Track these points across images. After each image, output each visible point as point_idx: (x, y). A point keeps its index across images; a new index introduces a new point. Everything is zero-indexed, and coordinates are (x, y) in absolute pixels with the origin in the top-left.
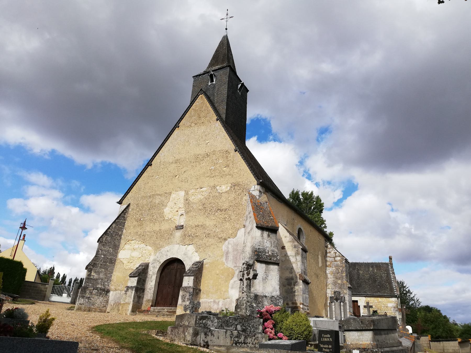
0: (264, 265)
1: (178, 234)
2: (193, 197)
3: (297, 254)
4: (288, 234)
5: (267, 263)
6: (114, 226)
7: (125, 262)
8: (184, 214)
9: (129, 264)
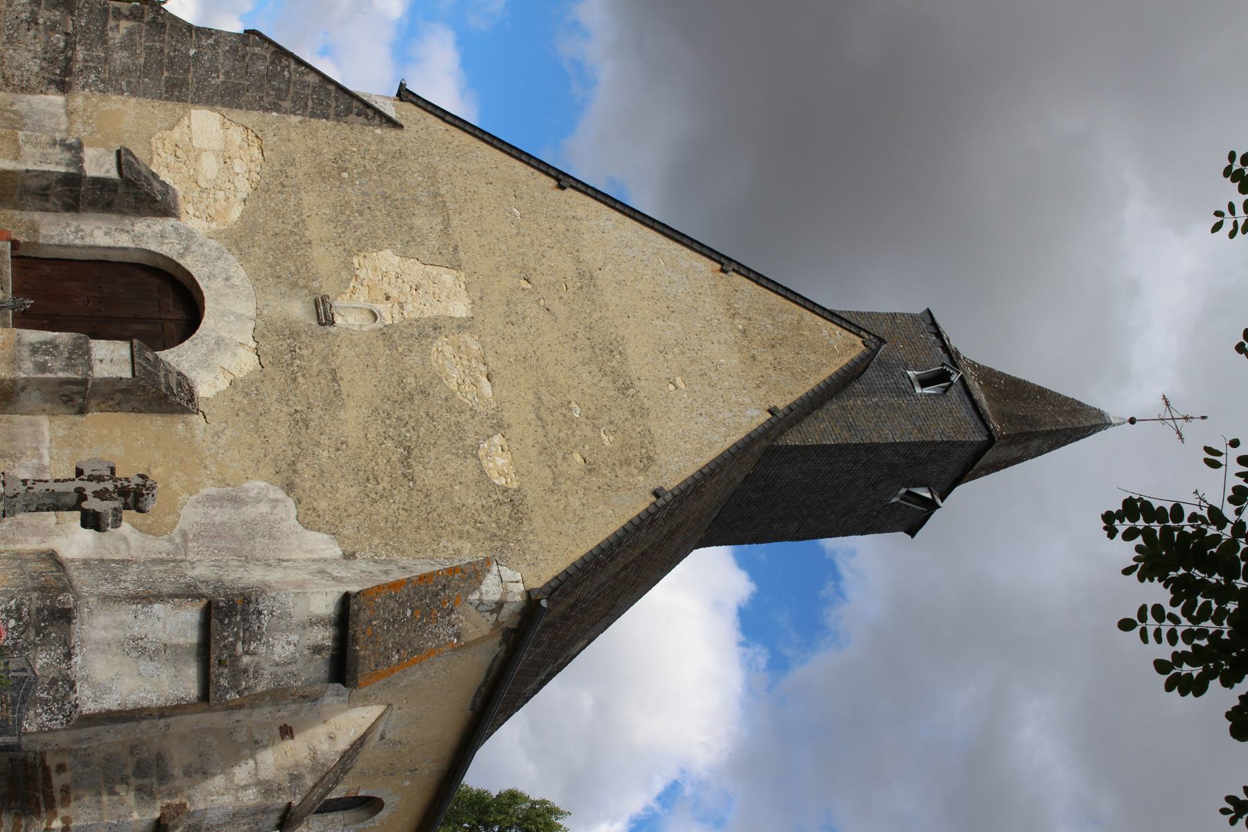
0: (192, 637)
1: (299, 310)
2: (448, 350)
3: (267, 788)
4: (343, 744)
5: (204, 651)
6: (312, 79)
7: (177, 134)
8: (378, 324)
9: (170, 147)
